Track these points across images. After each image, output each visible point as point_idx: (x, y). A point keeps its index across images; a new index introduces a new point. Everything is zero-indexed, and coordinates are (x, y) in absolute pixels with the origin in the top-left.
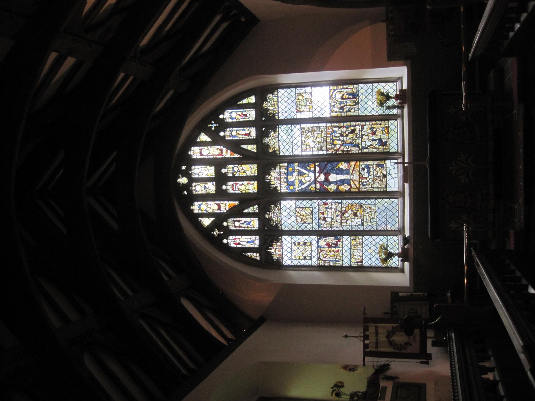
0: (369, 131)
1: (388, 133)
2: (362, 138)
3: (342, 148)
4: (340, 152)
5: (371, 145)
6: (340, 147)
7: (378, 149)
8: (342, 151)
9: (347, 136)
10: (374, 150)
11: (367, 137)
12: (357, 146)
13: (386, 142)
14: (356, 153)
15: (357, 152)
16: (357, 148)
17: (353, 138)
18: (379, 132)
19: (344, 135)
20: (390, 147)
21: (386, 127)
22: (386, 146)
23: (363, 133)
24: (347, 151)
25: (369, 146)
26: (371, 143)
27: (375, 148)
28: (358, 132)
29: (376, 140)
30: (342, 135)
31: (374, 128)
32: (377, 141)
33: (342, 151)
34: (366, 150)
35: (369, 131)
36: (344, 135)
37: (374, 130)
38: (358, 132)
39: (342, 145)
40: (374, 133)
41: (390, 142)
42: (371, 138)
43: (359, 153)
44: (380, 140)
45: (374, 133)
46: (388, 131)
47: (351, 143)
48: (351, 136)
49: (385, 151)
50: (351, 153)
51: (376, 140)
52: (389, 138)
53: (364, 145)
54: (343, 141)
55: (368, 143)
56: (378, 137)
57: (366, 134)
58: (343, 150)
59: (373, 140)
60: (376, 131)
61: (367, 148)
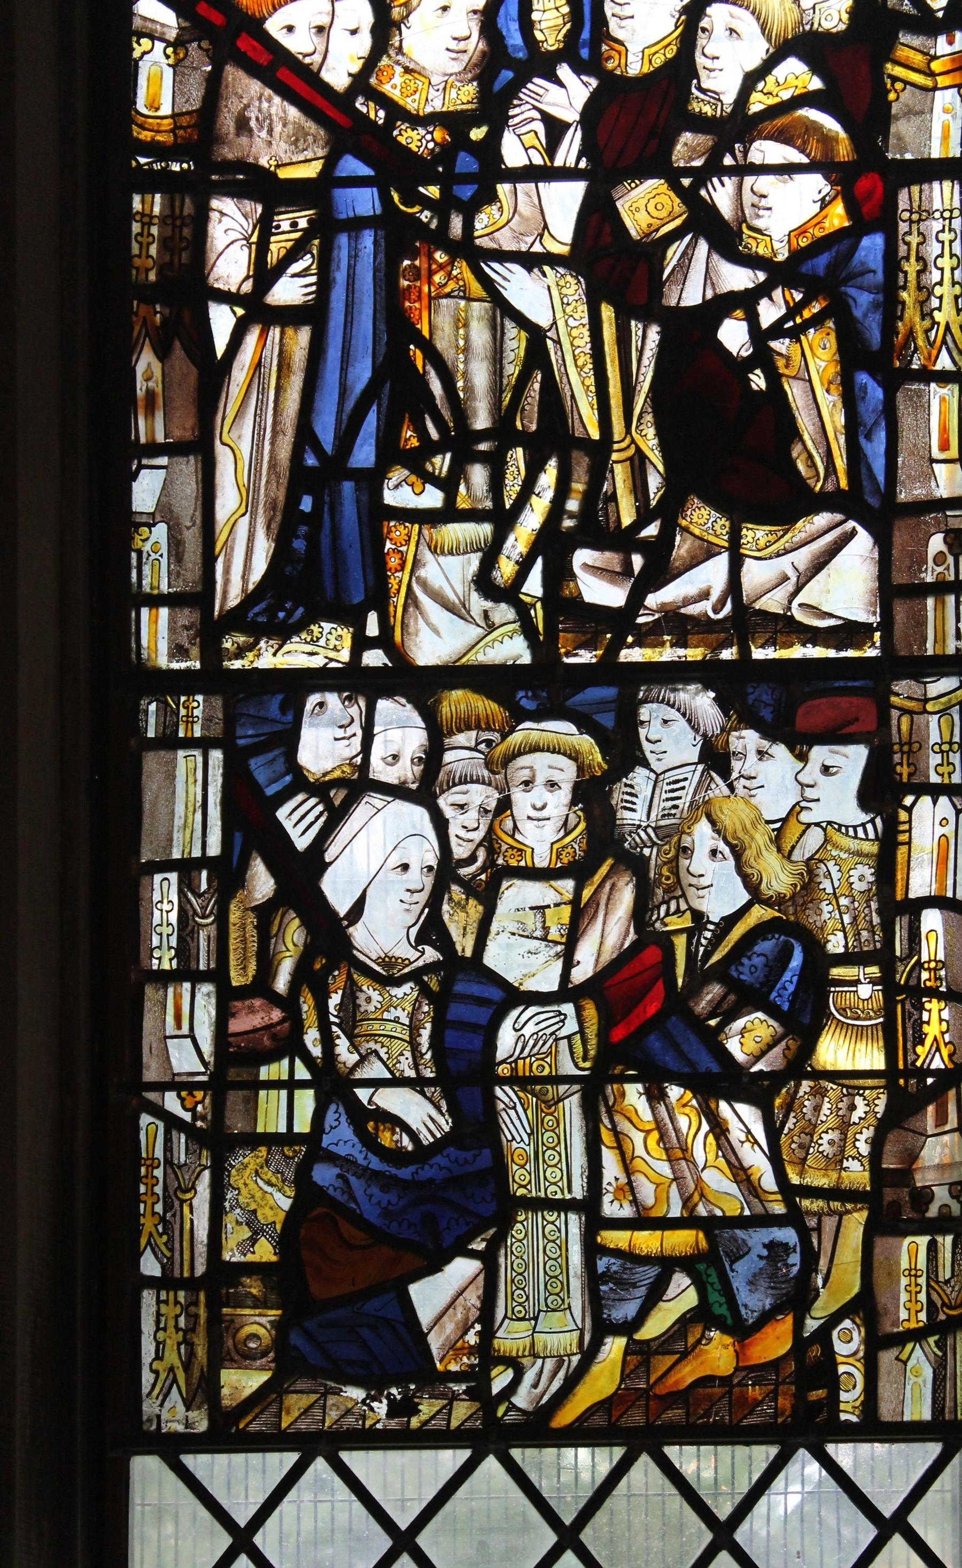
0: (718, 891)
1: (642, 1424)
2: (522, 692)
3: (280, 139)
4: (159, 86)
5: (330, 936)
6: (293, 78)
7: (220, 1143)
8: (201, 128)
9: (611, 265)
10: (183, 1035)
11: (544, 820)
12: (331, 560)
13: (399, 1356)
14: (122, 524)
15: (155, 569)
16: (246, 560)
17: (554, 436)
18: (687, 1154)
19: (644, 206)
20: (241, 1478)
21: (813, 1364)
22: (289, 1365)
23: (670, 733)
24: (189, 283)
25: (301, 874)
26: (384, 932)
27: (235, 1067)
28: (700, 585)
29: (464, 1072)
30: (642, 119)
31: (804, 1021)
32: (419, 1113)
33: (201, 128)
34: (187, 800)
35: (718, 891)
36: (644, 206)
37: (748, 1038)
38: (700, 585)
39: (349, 119)
40: (649, 1022)
41: (403, 1477)
42: (519, 957)
43: (120, 600)
44: (463, 1196)
45: (649, 1022)
46: (714, 1416)
47: (403, 381)
48: (597, 367)
49: (157, 1331)
50: (119, 398)
51: (464, 1072)
52: (496, 1435)
53: (322, 745)
54: (469, 164)
55: (377, 865)
56: (543, 1148)
57: (639, 804)
58: (205, 161)
59: (463, 996)
60: (721, 1081)
61: (250, 818)
